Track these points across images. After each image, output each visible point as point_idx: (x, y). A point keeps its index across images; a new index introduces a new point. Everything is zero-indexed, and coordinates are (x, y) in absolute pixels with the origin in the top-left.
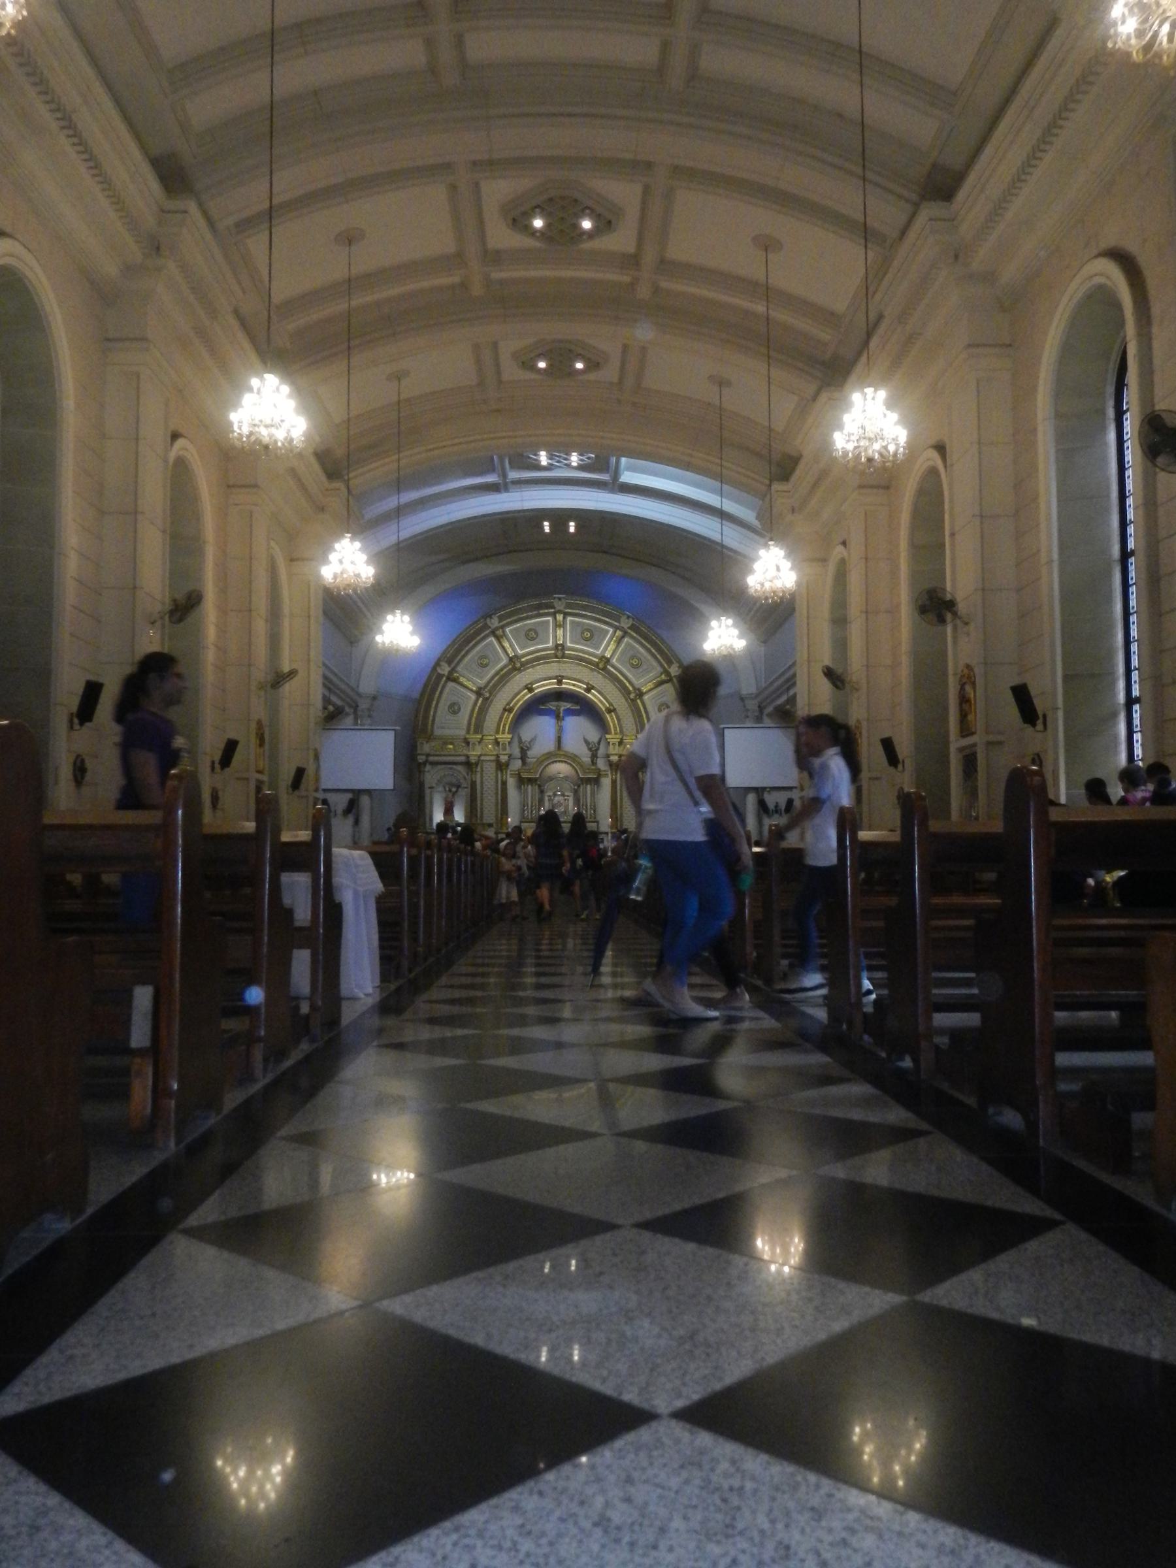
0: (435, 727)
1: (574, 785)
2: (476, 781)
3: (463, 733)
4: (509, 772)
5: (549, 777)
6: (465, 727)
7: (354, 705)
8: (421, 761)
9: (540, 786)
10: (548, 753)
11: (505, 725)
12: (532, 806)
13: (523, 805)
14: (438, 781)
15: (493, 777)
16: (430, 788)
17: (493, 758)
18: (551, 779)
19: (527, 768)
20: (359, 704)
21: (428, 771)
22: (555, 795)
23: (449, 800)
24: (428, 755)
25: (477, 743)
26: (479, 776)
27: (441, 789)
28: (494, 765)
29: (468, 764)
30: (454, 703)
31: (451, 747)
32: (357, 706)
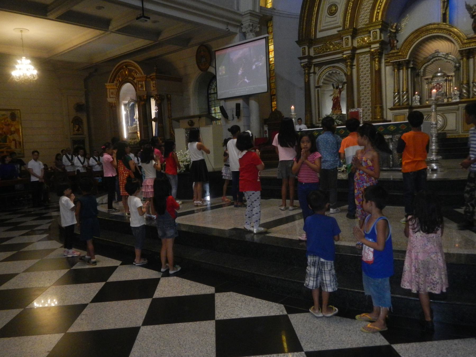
0: (318, 32)
1: (456, 63)
2: (351, 74)
3: (335, 32)
4: (383, 61)
5: (425, 58)
6: (341, 25)
7: (239, 24)
8: (302, 64)
9: (413, 69)
10: (417, 31)
11: (378, 13)
12: (403, 92)
13: (398, 91)
14: (325, 79)
15: (368, 68)
16: (317, 87)
17: (367, 49)
18: (427, 60)
19: (393, 51)
20: (243, 23)
21: (314, 73)
22: (435, 76)
23: (336, 96)
24: (310, 58)
25: (350, 37)
26: (355, 71)
27: (332, 88)
28: (368, 56)
29: (342, 60)
30: (331, 6)
31: (331, 47)
32: (242, 25)
